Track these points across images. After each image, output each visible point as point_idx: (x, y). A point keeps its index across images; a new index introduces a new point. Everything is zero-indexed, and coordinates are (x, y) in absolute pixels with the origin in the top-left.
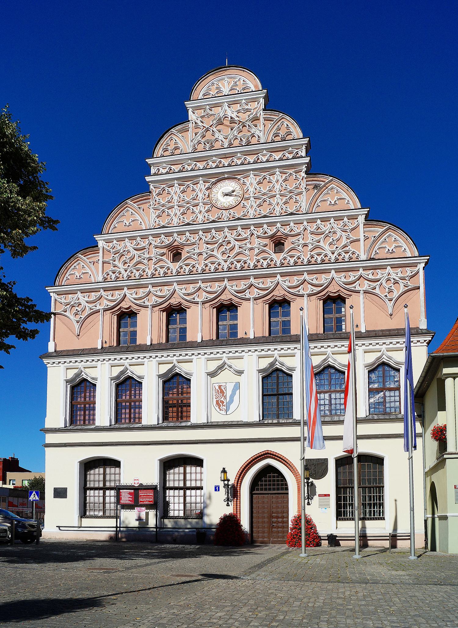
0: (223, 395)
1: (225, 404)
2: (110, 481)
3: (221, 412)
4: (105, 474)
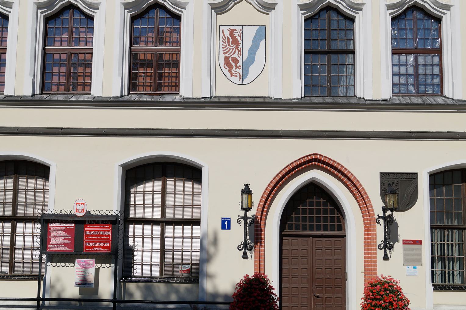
0: (237, 48)
1: (240, 64)
2: (26, 204)
3: (233, 79)
4: (16, 191)
